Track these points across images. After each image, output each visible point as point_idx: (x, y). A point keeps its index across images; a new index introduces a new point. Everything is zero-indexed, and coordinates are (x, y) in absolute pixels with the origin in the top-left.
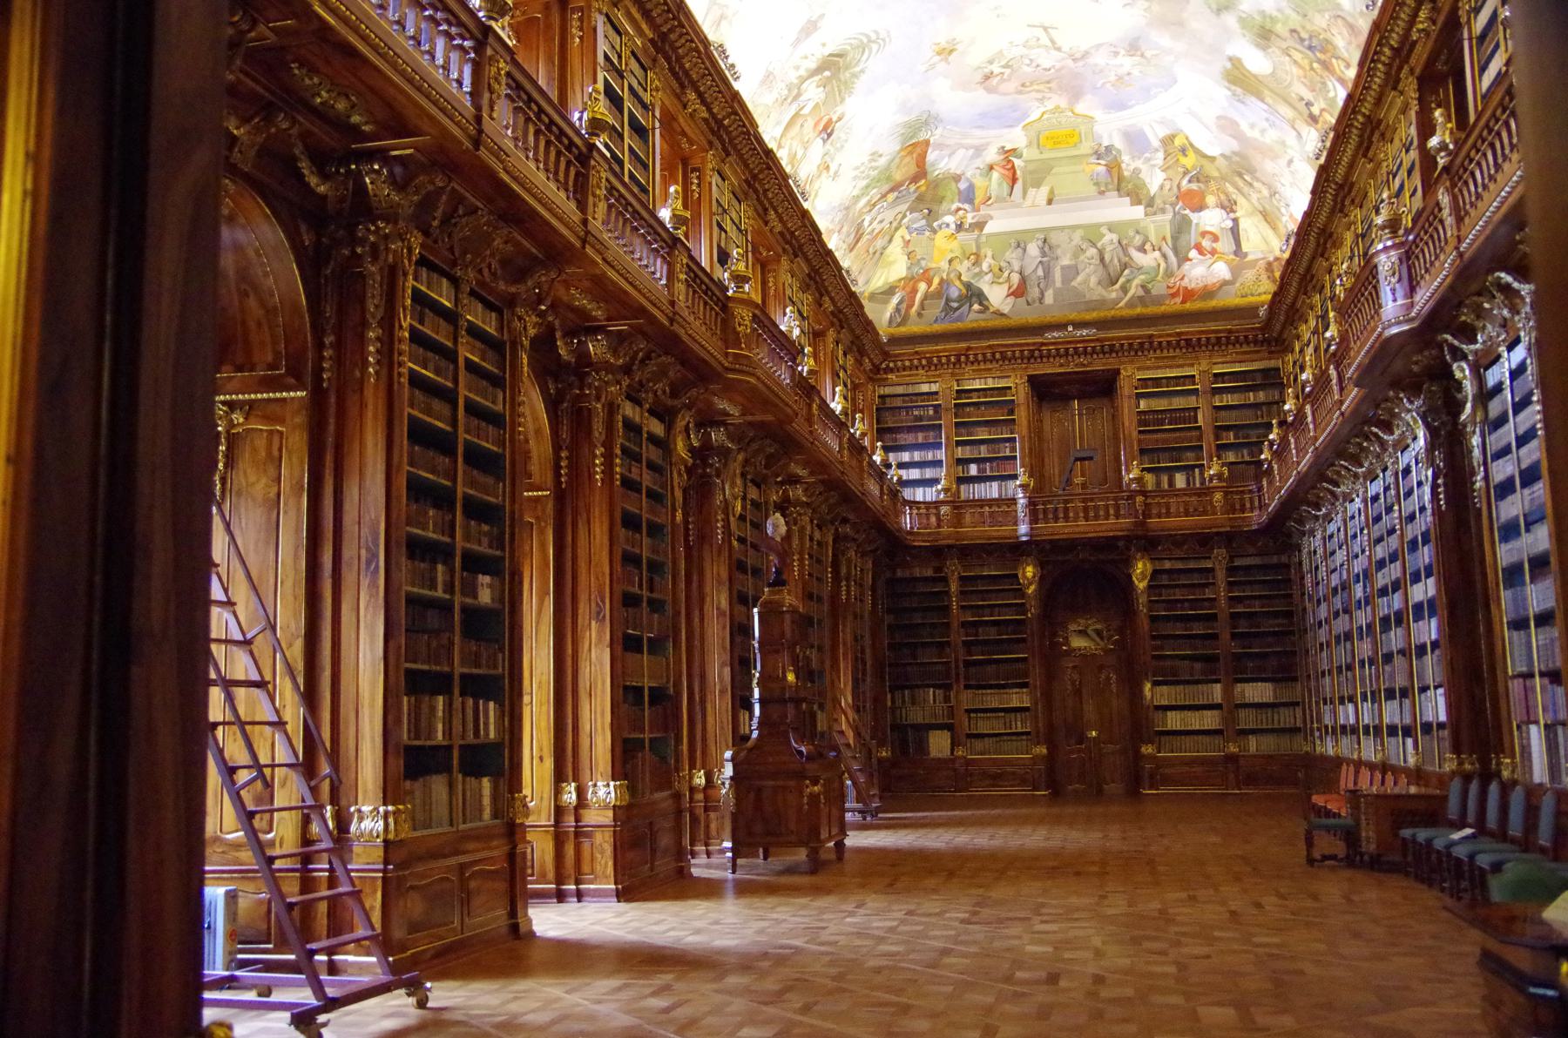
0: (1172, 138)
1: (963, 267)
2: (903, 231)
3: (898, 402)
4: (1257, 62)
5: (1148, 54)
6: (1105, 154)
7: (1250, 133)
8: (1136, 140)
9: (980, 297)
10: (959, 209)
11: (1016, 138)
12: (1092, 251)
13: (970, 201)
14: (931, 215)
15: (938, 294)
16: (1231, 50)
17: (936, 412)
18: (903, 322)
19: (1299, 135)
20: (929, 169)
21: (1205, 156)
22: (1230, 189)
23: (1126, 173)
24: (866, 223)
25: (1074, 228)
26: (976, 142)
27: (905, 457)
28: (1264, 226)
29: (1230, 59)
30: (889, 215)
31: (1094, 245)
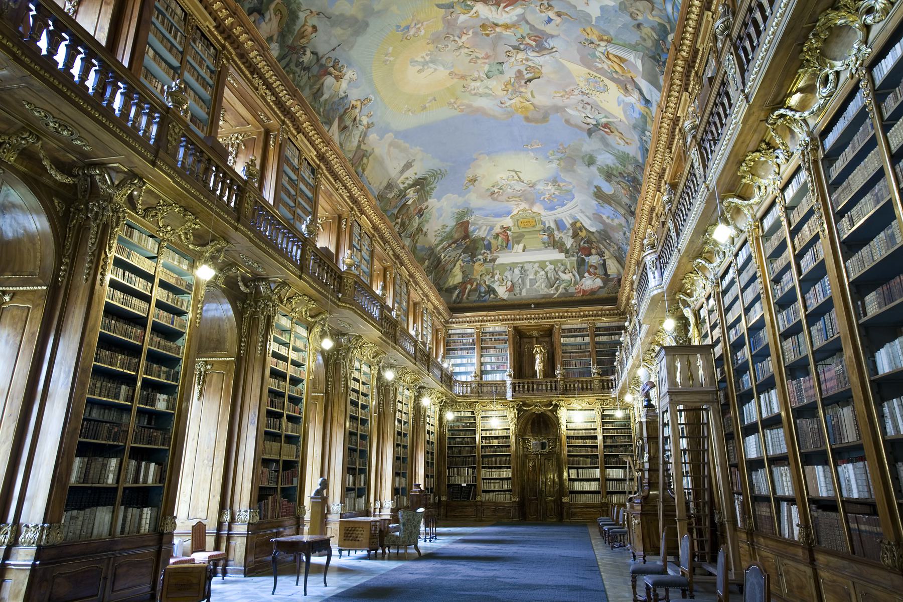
0: (575, 223)
1: (487, 278)
2: (460, 262)
3: (456, 338)
4: (608, 189)
5: (561, 184)
6: (548, 230)
7: (607, 221)
8: (560, 225)
9: (494, 291)
11: (508, 222)
14: (473, 256)
15: (475, 290)
16: (595, 184)
19: (627, 221)
25: (534, 262)
26: (491, 223)
27: (459, 361)
29: (596, 187)
30: (453, 254)
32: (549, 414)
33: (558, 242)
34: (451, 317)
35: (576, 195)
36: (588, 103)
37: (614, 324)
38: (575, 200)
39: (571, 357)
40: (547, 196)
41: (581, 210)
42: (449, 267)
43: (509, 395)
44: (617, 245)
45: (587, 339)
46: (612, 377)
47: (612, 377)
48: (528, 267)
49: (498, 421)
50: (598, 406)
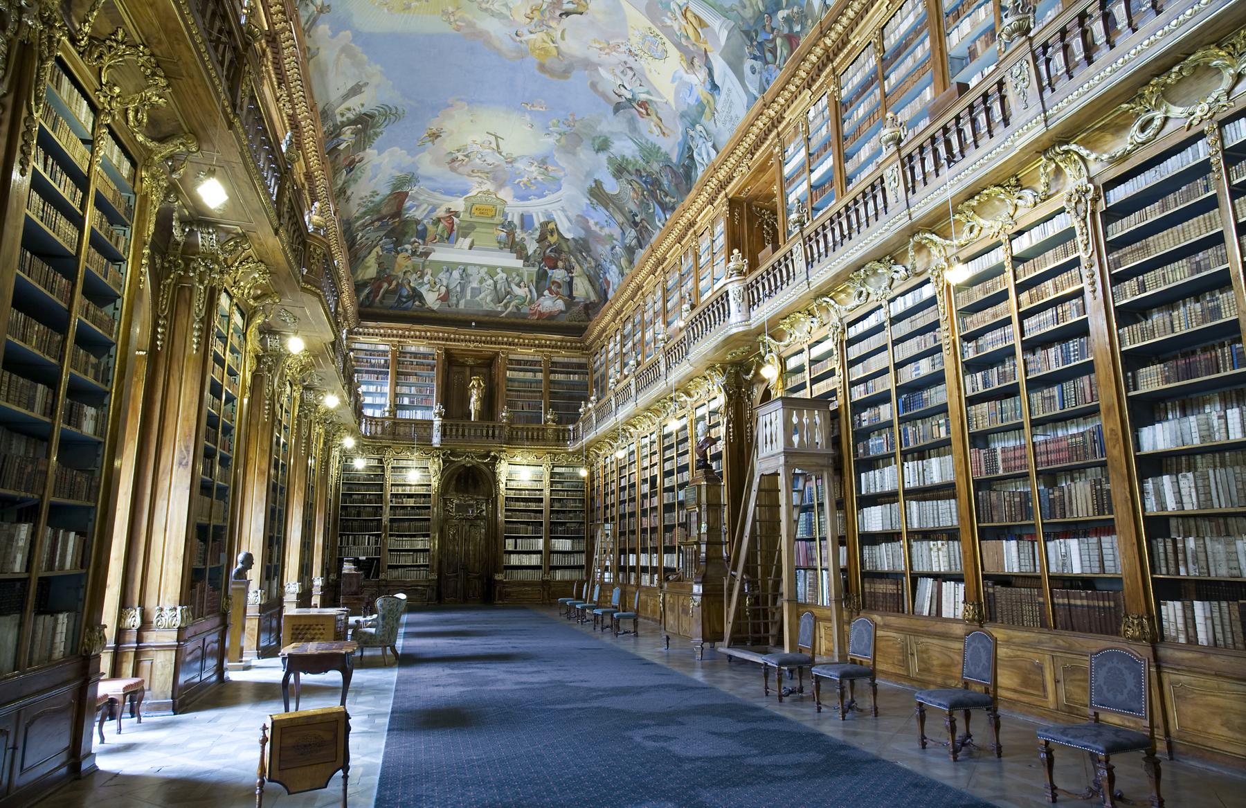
0: (547, 223)
2: (378, 249)
3: (361, 355)
4: (612, 186)
5: (550, 168)
6: (509, 227)
7: (593, 228)
8: (526, 221)
9: (420, 297)
11: (458, 204)
13: (424, 239)
14: (398, 243)
15: (394, 292)
18: (369, 306)
19: (623, 233)
25: (482, 266)
28: (586, 282)
29: (595, 181)
30: (373, 236)
32: (483, 467)
33: (517, 244)
34: (358, 325)
36: (631, 68)
37: (575, 360)
38: (560, 193)
39: (519, 397)
40: (525, 179)
41: (563, 208)
42: (363, 253)
43: (436, 440)
44: (596, 261)
45: (540, 376)
46: (571, 427)
47: (571, 427)
48: (472, 268)
49: (417, 474)
50: (547, 460)
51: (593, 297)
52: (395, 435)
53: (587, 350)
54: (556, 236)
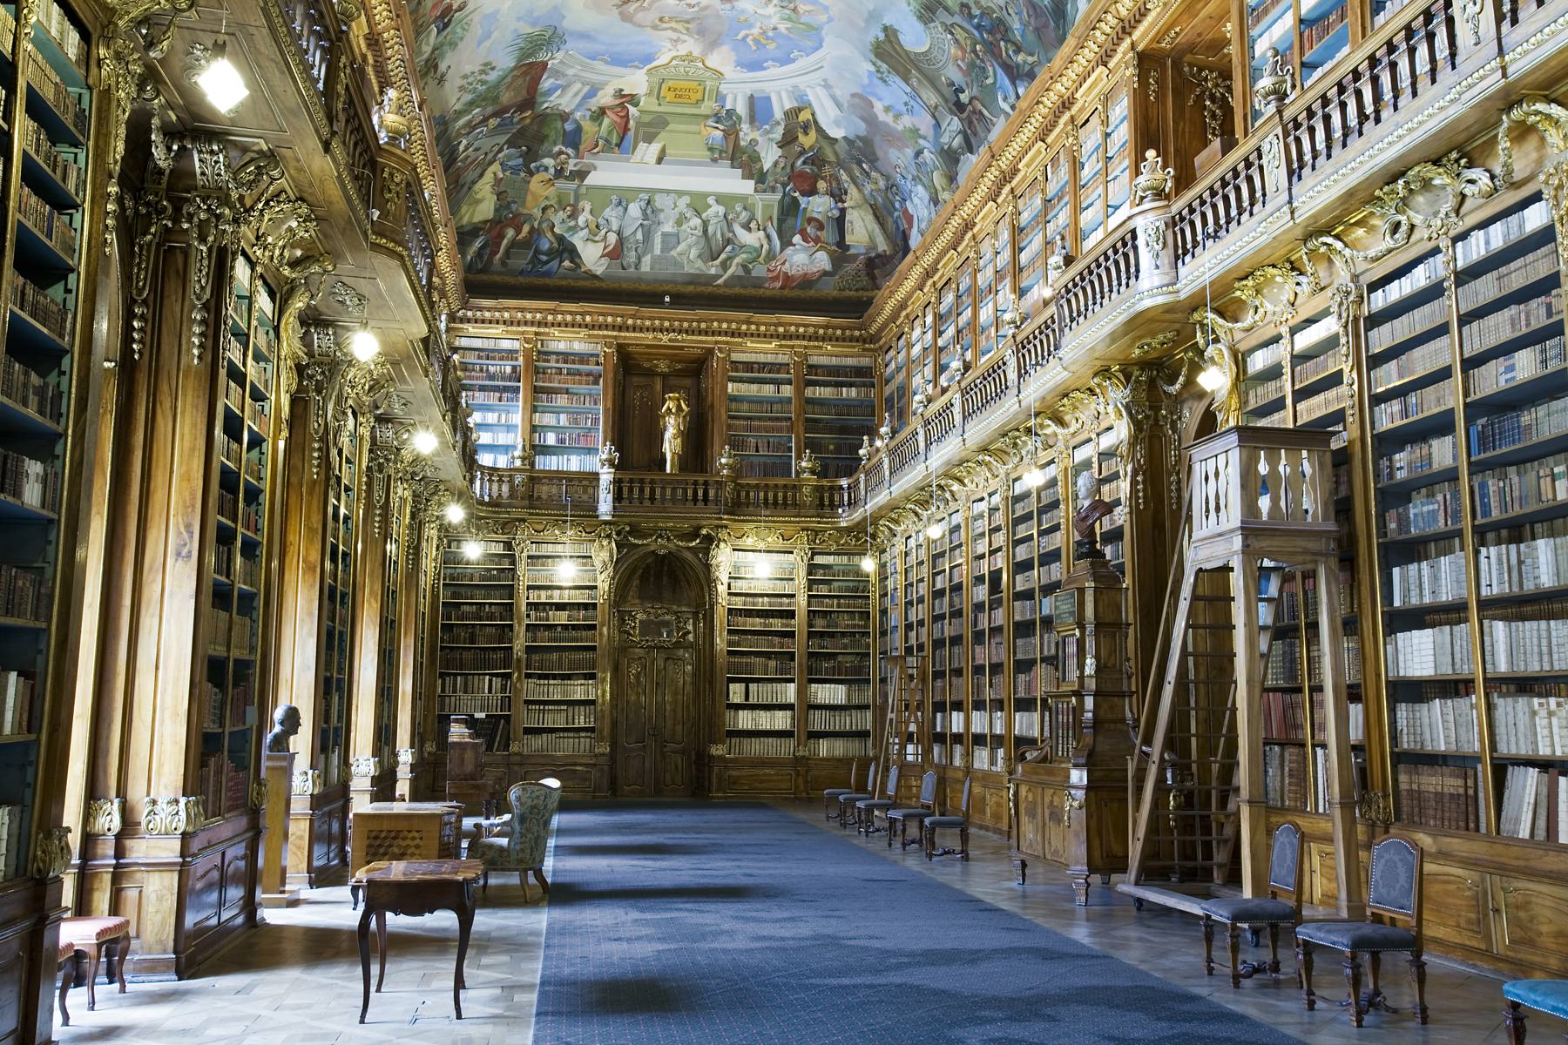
0: (798, 110)
1: (558, 218)
2: (496, 167)
5: (802, 8)
6: (727, 120)
7: (882, 117)
8: (758, 109)
9: (573, 253)
10: (561, 153)
11: (637, 81)
12: (696, 221)
14: (531, 155)
15: (526, 244)
16: (887, 21)
17: (514, 368)
18: (483, 271)
19: (938, 125)
20: (540, 99)
21: (826, 137)
22: (844, 177)
23: (742, 143)
24: (461, 148)
25: (680, 193)
28: (870, 218)
29: (886, 29)
30: (487, 144)
31: (699, 215)
32: (689, 556)
35: (828, 40)
37: (850, 361)
40: (756, 31)
42: (470, 175)
43: (605, 507)
44: (887, 178)
45: (787, 391)
46: (844, 482)
48: (664, 197)
49: (572, 569)
50: (802, 544)
51: (882, 246)
52: (535, 499)
53: (872, 342)
54: (813, 134)
